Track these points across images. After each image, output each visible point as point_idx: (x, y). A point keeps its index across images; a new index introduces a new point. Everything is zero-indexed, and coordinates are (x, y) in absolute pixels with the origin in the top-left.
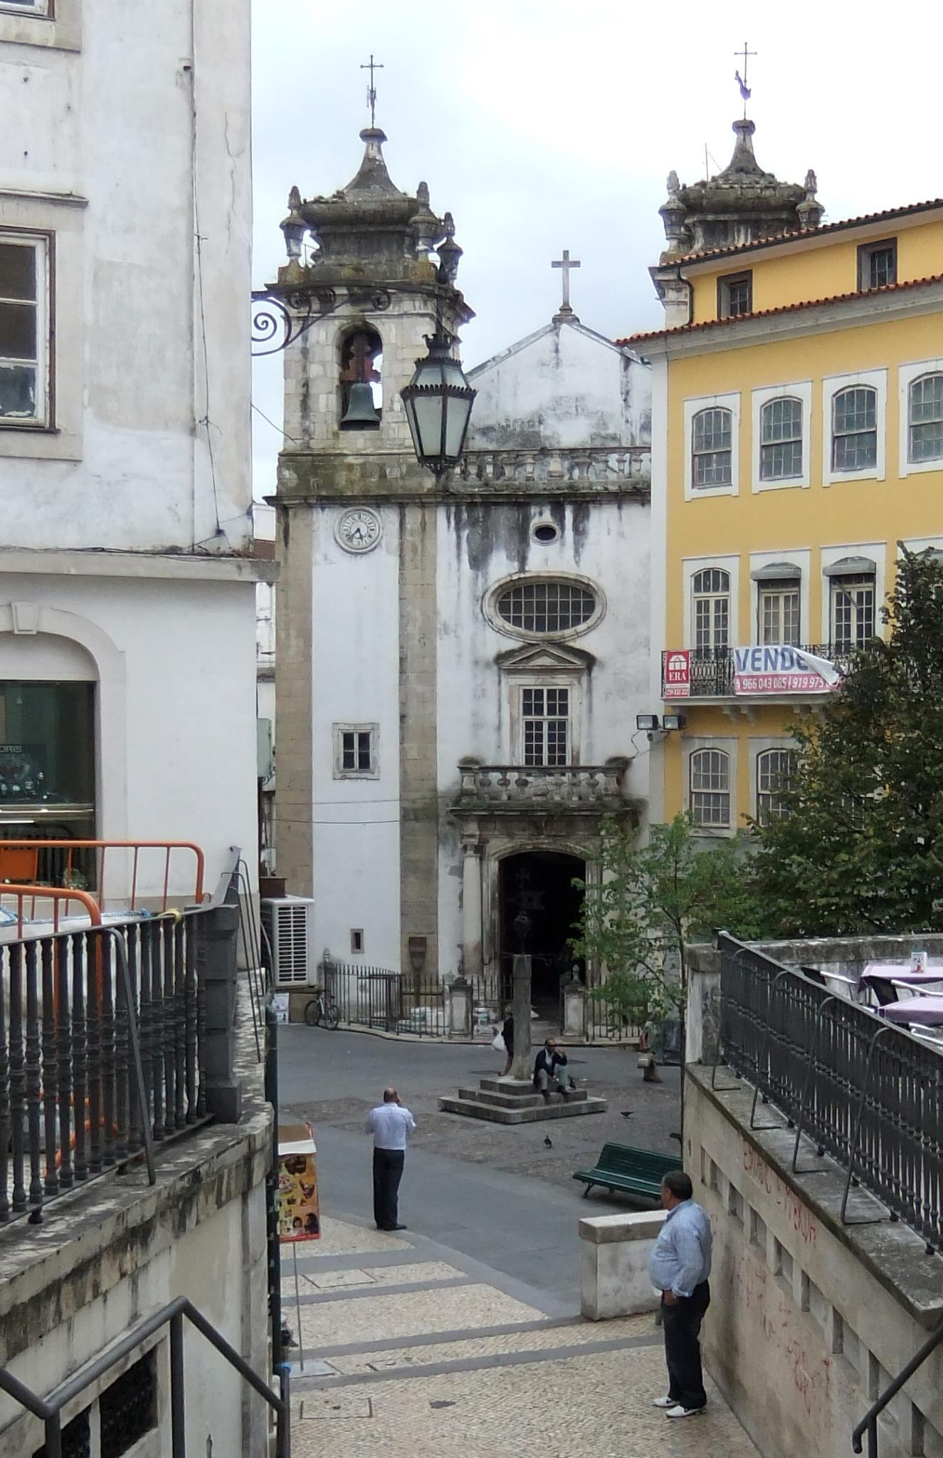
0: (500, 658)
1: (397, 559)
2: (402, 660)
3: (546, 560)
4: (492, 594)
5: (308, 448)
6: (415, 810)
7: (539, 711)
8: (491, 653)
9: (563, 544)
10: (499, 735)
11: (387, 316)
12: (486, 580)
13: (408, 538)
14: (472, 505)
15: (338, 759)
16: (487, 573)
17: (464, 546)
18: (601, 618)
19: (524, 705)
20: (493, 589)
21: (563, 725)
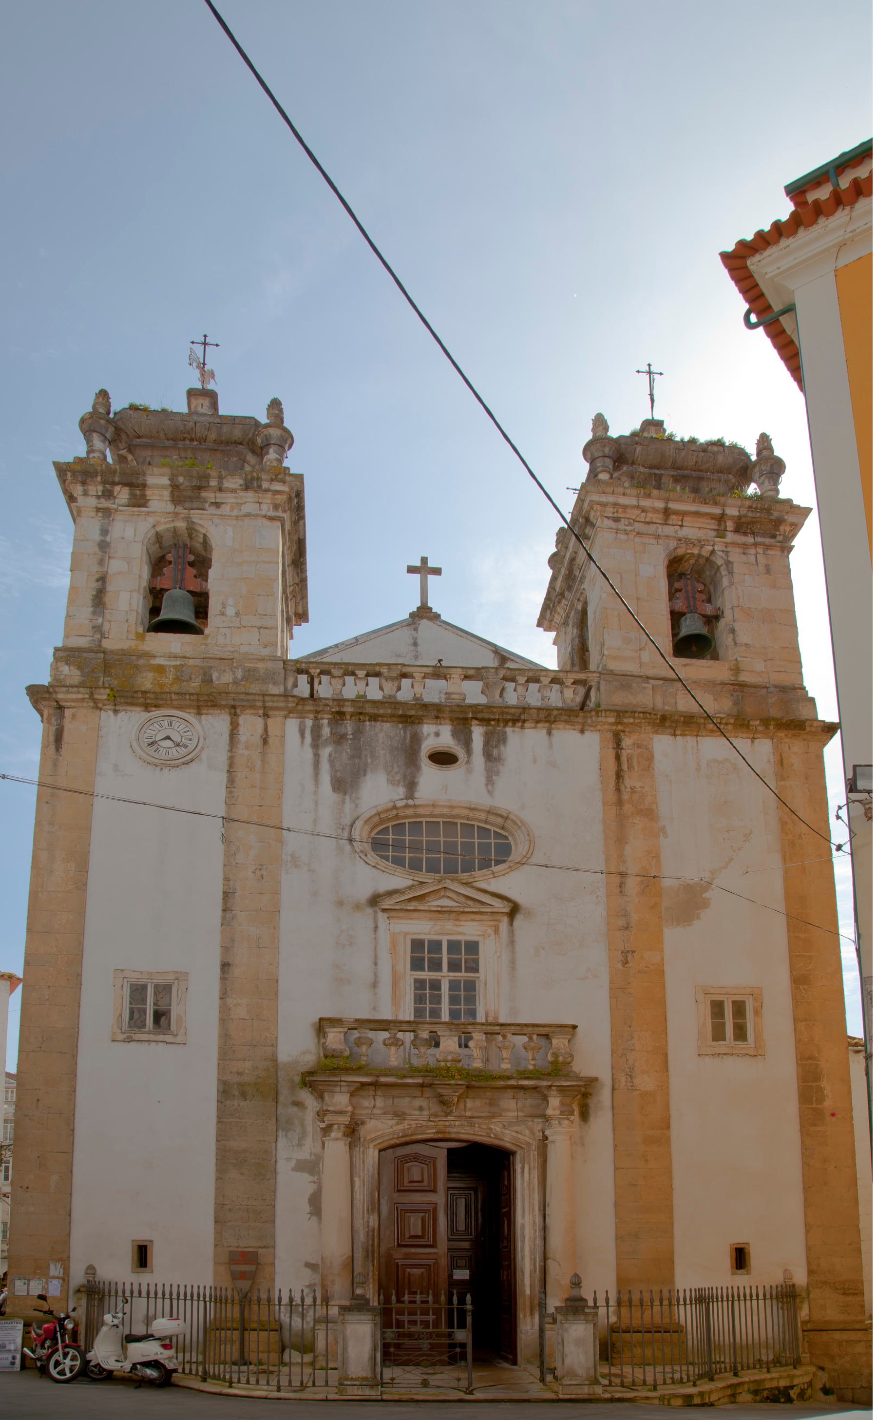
0: (374, 901)
1: (223, 777)
2: (226, 895)
4: (366, 822)
6: (241, 1085)
7: (436, 966)
8: (365, 893)
9: (469, 771)
10: (375, 994)
12: (357, 806)
13: (241, 750)
15: (121, 1015)
16: (358, 798)
17: (325, 766)
19: (413, 959)
20: (367, 815)
21: (471, 986)
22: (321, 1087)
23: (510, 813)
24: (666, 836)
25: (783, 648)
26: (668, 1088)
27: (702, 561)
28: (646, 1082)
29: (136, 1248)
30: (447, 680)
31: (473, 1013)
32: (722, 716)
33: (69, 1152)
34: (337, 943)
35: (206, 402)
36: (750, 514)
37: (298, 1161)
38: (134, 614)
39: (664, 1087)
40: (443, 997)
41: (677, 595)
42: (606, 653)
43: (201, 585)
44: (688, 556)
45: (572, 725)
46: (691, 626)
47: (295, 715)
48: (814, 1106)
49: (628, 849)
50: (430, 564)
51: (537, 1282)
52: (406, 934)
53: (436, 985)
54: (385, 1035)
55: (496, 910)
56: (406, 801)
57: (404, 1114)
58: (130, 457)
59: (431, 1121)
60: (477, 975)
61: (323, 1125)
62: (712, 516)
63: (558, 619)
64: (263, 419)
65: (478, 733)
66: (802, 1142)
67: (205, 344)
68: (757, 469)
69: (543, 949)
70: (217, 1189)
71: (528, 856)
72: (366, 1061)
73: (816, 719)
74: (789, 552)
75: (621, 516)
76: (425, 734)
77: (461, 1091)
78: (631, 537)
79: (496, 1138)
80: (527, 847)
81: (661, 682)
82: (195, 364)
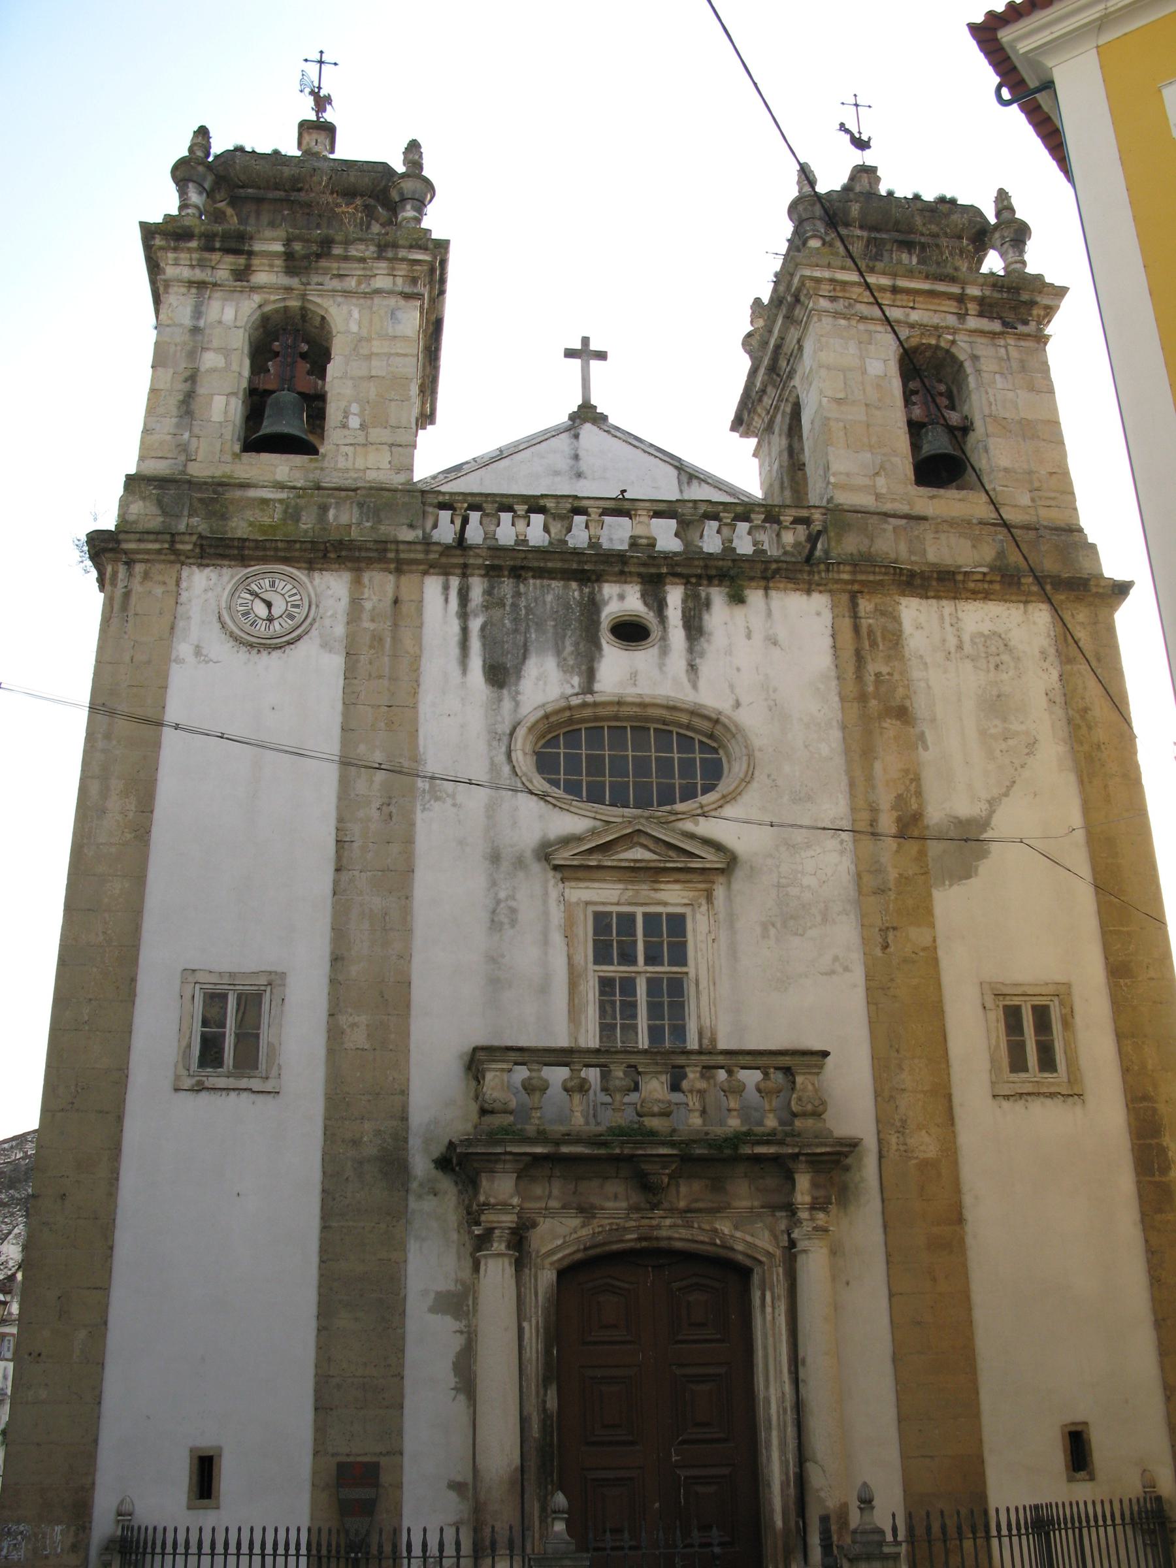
0: (545, 852)
3: (634, 675)
4: (530, 729)
5: (184, 472)
7: (628, 957)
9: (664, 651)
11: (347, 293)
12: (517, 704)
14: (492, 572)
15: (189, 1046)
16: (518, 693)
17: (475, 645)
18: (748, 779)
20: (532, 719)
21: (677, 986)
22: (476, 1165)
23: (720, 713)
24: (926, 748)
25: (1051, 474)
26: (956, 1152)
27: (940, 354)
28: (926, 1145)
29: (196, 1461)
30: (631, 518)
31: (680, 1031)
32: (985, 570)
33: (104, 1289)
34: (493, 921)
35: (322, 137)
36: (996, 295)
37: (438, 1293)
38: (230, 428)
39: (950, 1150)
40: (639, 1007)
41: (914, 398)
42: (832, 480)
43: (316, 384)
44: (923, 347)
45: (794, 583)
46: (937, 443)
47: (437, 570)
48: (1157, 1179)
49: (878, 766)
50: (594, 346)
51: (792, 1506)
52: (587, 903)
53: (628, 985)
54: (562, 1073)
55: (708, 866)
56: (582, 696)
57: (593, 1207)
58: (230, 211)
59: (631, 1219)
60: (684, 969)
61: (477, 1231)
62: (950, 296)
63: (758, 423)
64: (400, 168)
65: (675, 596)
66: (1147, 1241)
67: (321, 62)
68: (997, 235)
69: (773, 925)
70: (319, 1348)
71: (747, 780)
72: (539, 1118)
73: (1100, 576)
74: (1046, 344)
75: (840, 294)
76: (606, 597)
77: (674, 1167)
78: (854, 323)
79: (724, 1247)
80: (744, 766)
81: (904, 522)
82: (307, 90)
